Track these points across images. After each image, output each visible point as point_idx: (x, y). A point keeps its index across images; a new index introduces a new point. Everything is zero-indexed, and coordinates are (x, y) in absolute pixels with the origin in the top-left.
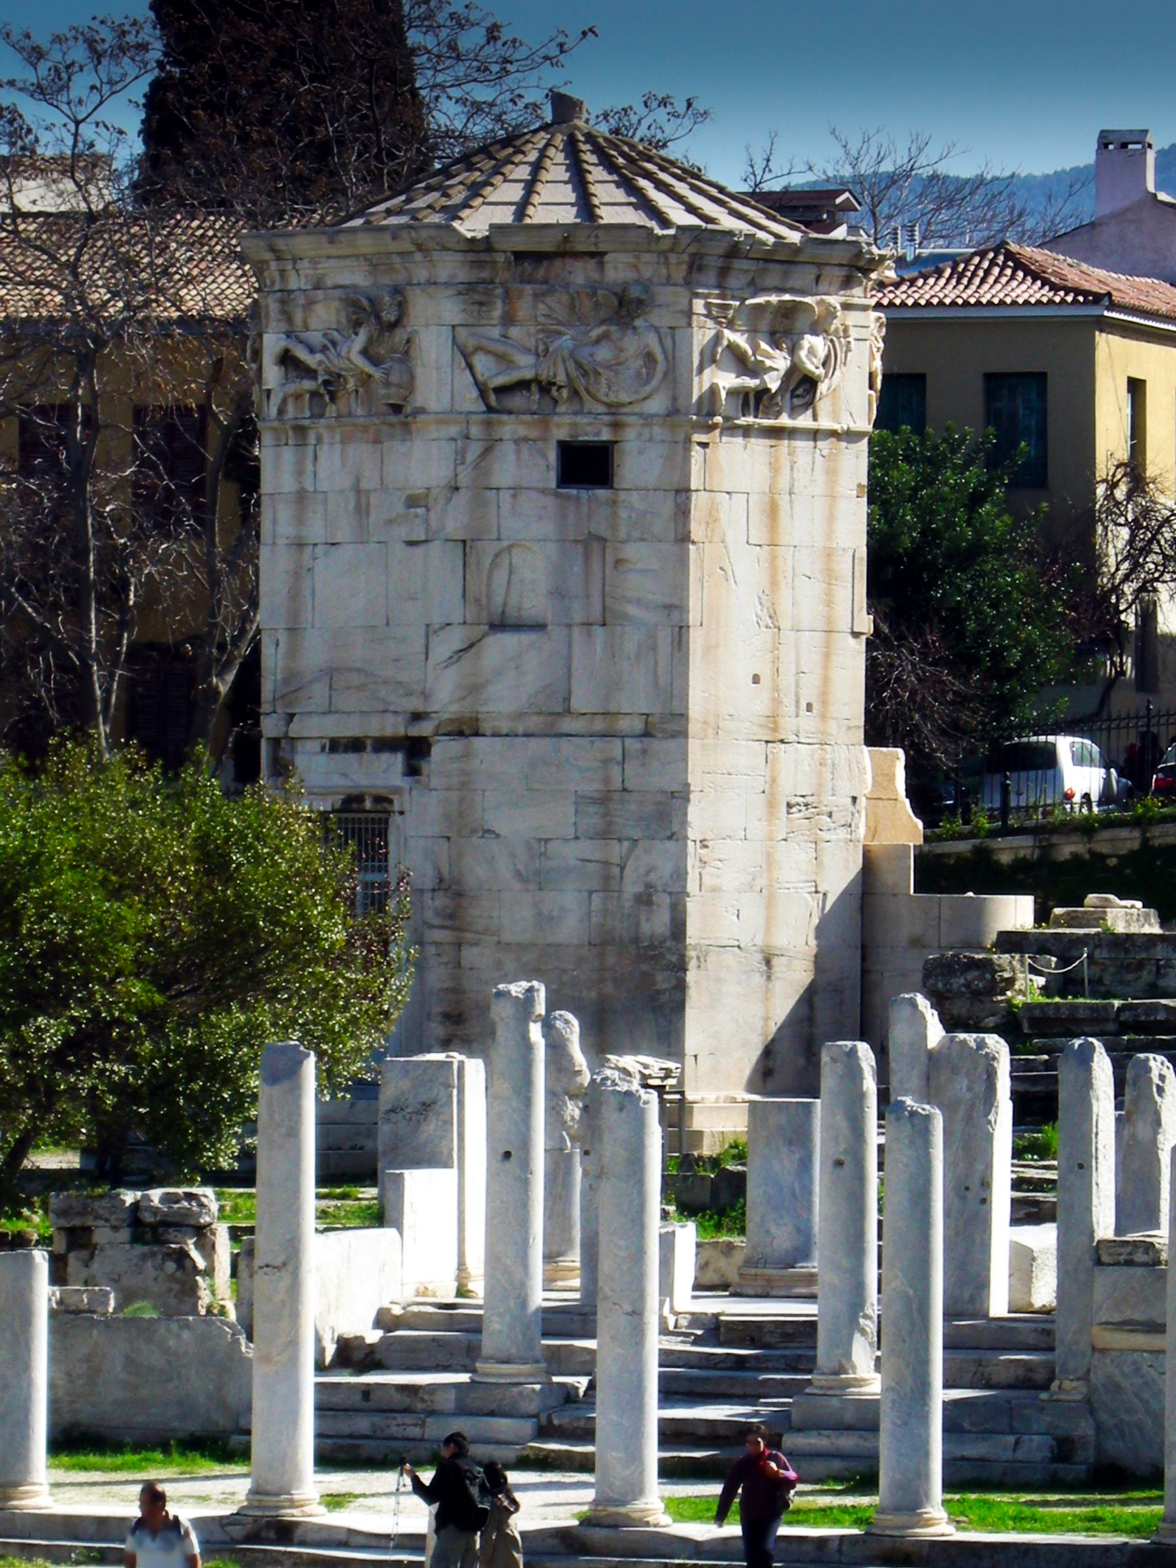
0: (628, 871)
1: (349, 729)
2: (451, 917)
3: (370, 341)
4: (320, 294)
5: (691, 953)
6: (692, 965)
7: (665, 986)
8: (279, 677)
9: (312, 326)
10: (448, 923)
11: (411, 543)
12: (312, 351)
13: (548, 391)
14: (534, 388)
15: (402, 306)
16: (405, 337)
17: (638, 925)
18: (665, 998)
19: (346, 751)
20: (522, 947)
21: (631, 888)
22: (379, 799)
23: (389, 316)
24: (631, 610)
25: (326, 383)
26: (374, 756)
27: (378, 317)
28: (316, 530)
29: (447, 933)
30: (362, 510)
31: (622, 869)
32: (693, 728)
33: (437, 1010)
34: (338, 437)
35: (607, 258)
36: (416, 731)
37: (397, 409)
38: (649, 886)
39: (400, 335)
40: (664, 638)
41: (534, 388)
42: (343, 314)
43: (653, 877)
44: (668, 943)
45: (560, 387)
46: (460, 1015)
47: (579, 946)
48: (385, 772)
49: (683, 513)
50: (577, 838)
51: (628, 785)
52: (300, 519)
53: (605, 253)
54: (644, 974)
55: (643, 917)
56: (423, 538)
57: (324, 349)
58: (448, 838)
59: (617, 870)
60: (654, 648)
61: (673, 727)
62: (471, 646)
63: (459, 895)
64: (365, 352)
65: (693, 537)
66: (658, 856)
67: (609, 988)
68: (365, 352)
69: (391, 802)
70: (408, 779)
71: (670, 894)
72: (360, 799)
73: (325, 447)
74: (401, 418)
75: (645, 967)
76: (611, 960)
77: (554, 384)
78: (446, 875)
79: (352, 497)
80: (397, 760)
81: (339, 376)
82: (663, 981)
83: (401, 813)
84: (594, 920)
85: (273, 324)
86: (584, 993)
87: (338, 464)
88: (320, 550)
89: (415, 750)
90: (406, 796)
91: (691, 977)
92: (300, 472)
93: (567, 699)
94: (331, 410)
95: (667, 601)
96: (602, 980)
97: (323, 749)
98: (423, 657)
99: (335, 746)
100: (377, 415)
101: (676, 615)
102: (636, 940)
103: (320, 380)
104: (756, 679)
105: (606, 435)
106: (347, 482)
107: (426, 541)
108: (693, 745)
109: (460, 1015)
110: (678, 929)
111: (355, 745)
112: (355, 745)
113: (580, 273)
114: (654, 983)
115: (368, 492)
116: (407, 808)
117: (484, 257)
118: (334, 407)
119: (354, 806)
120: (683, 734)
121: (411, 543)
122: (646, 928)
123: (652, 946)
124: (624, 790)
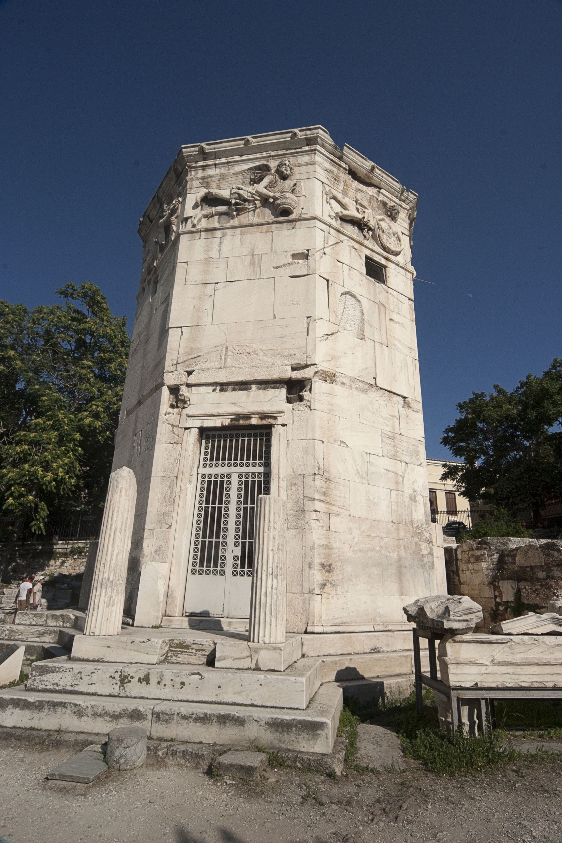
0: (405, 479)
2: (324, 494)
8: (182, 351)
10: (323, 498)
16: (292, 184)
18: (426, 560)
19: (234, 390)
20: (362, 520)
22: (263, 416)
24: (397, 343)
26: (261, 392)
29: (322, 505)
31: (403, 478)
33: (317, 561)
35: (382, 191)
36: (297, 375)
38: (415, 491)
39: (288, 184)
45: (370, 229)
46: (330, 565)
50: (383, 456)
51: (402, 432)
53: (380, 189)
54: (417, 544)
58: (323, 442)
59: (401, 479)
60: (406, 365)
62: (332, 334)
63: (328, 480)
67: (402, 553)
71: (423, 496)
72: (247, 416)
75: (416, 540)
76: (402, 534)
77: (368, 226)
78: (322, 466)
81: (245, 200)
84: (393, 507)
86: (392, 554)
89: (296, 388)
93: (375, 378)
96: (399, 546)
102: (412, 522)
105: (383, 261)
106: (245, 251)
107: (308, 275)
109: (330, 565)
111: (244, 385)
112: (244, 385)
113: (371, 191)
114: (421, 550)
117: (337, 160)
119: (241, 422)
124: (401, 434)
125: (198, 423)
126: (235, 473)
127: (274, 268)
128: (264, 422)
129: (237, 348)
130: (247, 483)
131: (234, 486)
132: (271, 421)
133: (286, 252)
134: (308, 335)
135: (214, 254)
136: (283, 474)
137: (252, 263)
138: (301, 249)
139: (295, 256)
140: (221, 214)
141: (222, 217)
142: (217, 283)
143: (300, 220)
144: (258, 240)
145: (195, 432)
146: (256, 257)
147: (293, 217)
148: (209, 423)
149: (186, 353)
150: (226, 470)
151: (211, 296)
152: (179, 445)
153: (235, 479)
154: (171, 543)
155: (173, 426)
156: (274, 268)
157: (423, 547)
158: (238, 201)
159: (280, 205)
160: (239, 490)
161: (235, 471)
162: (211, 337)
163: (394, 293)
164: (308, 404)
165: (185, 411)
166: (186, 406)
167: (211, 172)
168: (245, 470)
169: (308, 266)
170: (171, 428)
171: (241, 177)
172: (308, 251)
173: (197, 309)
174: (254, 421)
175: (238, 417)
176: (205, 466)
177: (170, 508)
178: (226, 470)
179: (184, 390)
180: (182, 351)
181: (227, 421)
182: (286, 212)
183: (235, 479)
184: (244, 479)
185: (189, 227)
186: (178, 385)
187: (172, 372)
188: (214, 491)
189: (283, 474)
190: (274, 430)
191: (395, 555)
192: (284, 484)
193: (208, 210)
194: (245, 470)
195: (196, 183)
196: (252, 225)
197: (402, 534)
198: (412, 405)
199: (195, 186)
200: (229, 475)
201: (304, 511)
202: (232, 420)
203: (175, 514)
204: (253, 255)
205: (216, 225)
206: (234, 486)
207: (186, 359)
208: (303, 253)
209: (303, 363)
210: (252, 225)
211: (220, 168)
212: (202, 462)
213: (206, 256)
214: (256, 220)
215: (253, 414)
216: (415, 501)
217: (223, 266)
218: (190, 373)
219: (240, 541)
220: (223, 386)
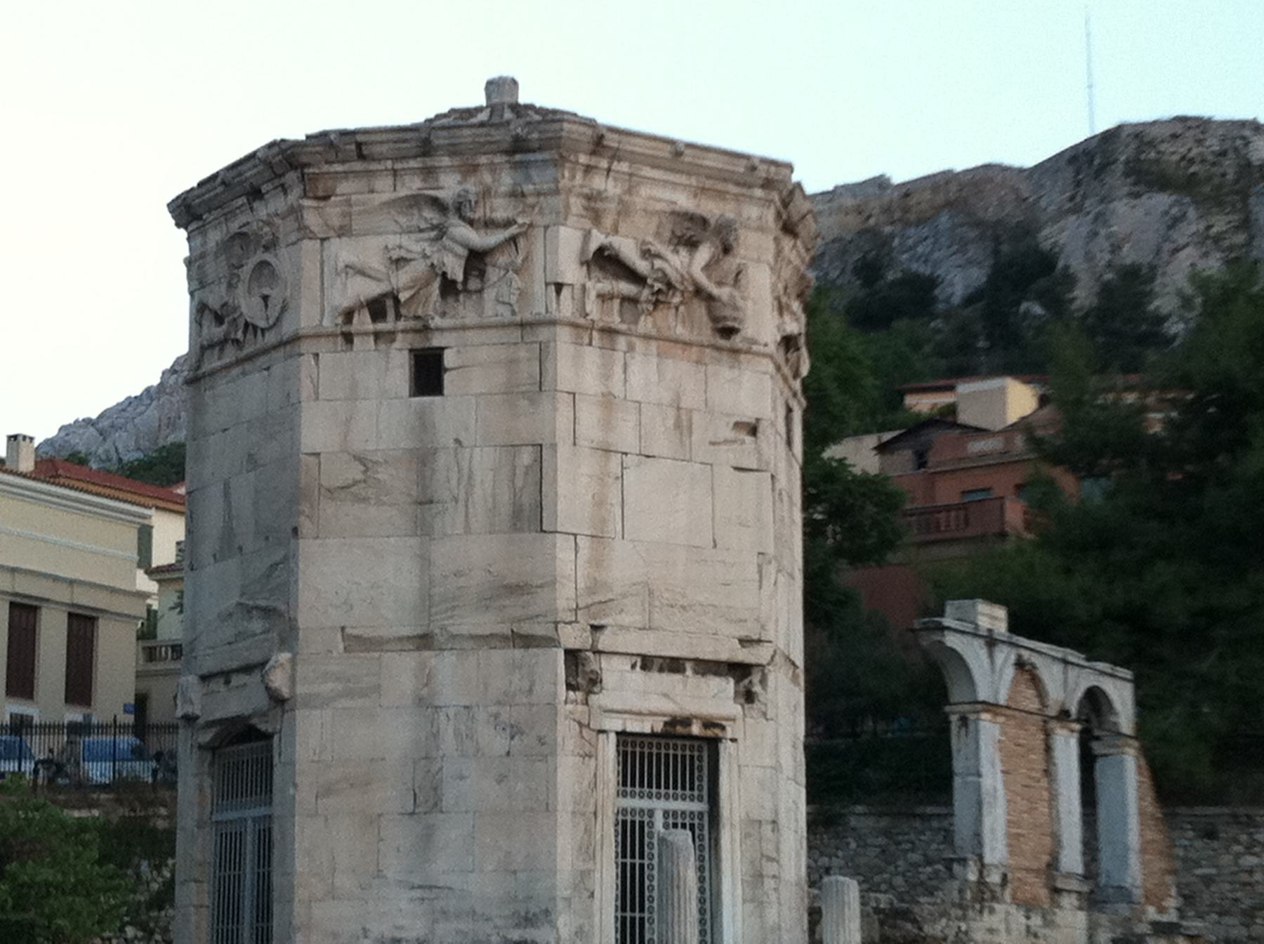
8: (581, 585)
19: (661, 670)
22: (708, 724)
26: (699, 679)
28: (626, 437)
30: (682, 427)
48: (713, 698)
52: (607, 424)
56: (755, 467)
69: (723, 728)
72: (687, 721)
73: (638, 358)
79: (671, 413)
80: (728, 686)
83: (734, 740)
85: (572, 220)
87: (655, 378)
88: (628, 460)
90: (739, 722)
92: (606, 376)
97: (633, 666)
98: (757, 584)
99: (647, 662)
106: (667, 397)
107: (757, 470)
111: (674, 665)
112: (674, 665)
115: (690, 411)
116: (739, 736)
119: (679, 729)
125: (615, 724)
127: (713, 443)
128: (709, 733)
129: (666, 595)
132: (717, 731)
133: (728, 415)
134: (760, 587)
135: (618, 389)
136: (736, 819)
137: (678, 426)
138: (749, 417)
139: (738, 425)
140: (628, 300)
141: (626, 304)
142: (626, 454)
143: (748, 352)
144: (680, 369)
145: (613, 737)
146: (683, 412)
147: (737, 341)
148: (634, 726)
149: (591, 590)
150: (644, 804)
151: (617, 478)
152: (593, 759)
154: (597, 919)
155: (580, 724)
156: (713, 443)
159: (725, 318)
162: (624, 566)
164: (763, 708)
165: (593, 699)
166: (596, 689)
167: (598, 182)
169: (759, 452)
170: (577, 726)
171: (655, 220)
172: (758, 420)
173: (600, 502)
174: (696, 729)
175: (674, 722)
176: (625, 795)
177: (590, 865)
178: (644, 804)
179: (593, 663)
180: (581, 585)
181: (659, 728)
182: (728, 332)
185: (566, 307)
186: (580, 650)
187: (570, 623)
188: (632, 835)
189: (736, 819)
190: (722, 747)
192: (737, 837)
193: (606, 285)
195: (576, 204)
196: (676, 341)
199: (574, 210)
200: (651, 813)
201: (761, 876)
202: (666, 724)
203: (598, 875)
204: (679, 408)
205: (615, 320)
207: (590, 601)
208: (748, 424)
209: (756, 637)
210: (676, 341)
211: (615, 179)
213: (605, 390)
214: (681, 331)
215: (696, 717)
217: (632, 418)
218: (596, 628)
220: (647, 662)
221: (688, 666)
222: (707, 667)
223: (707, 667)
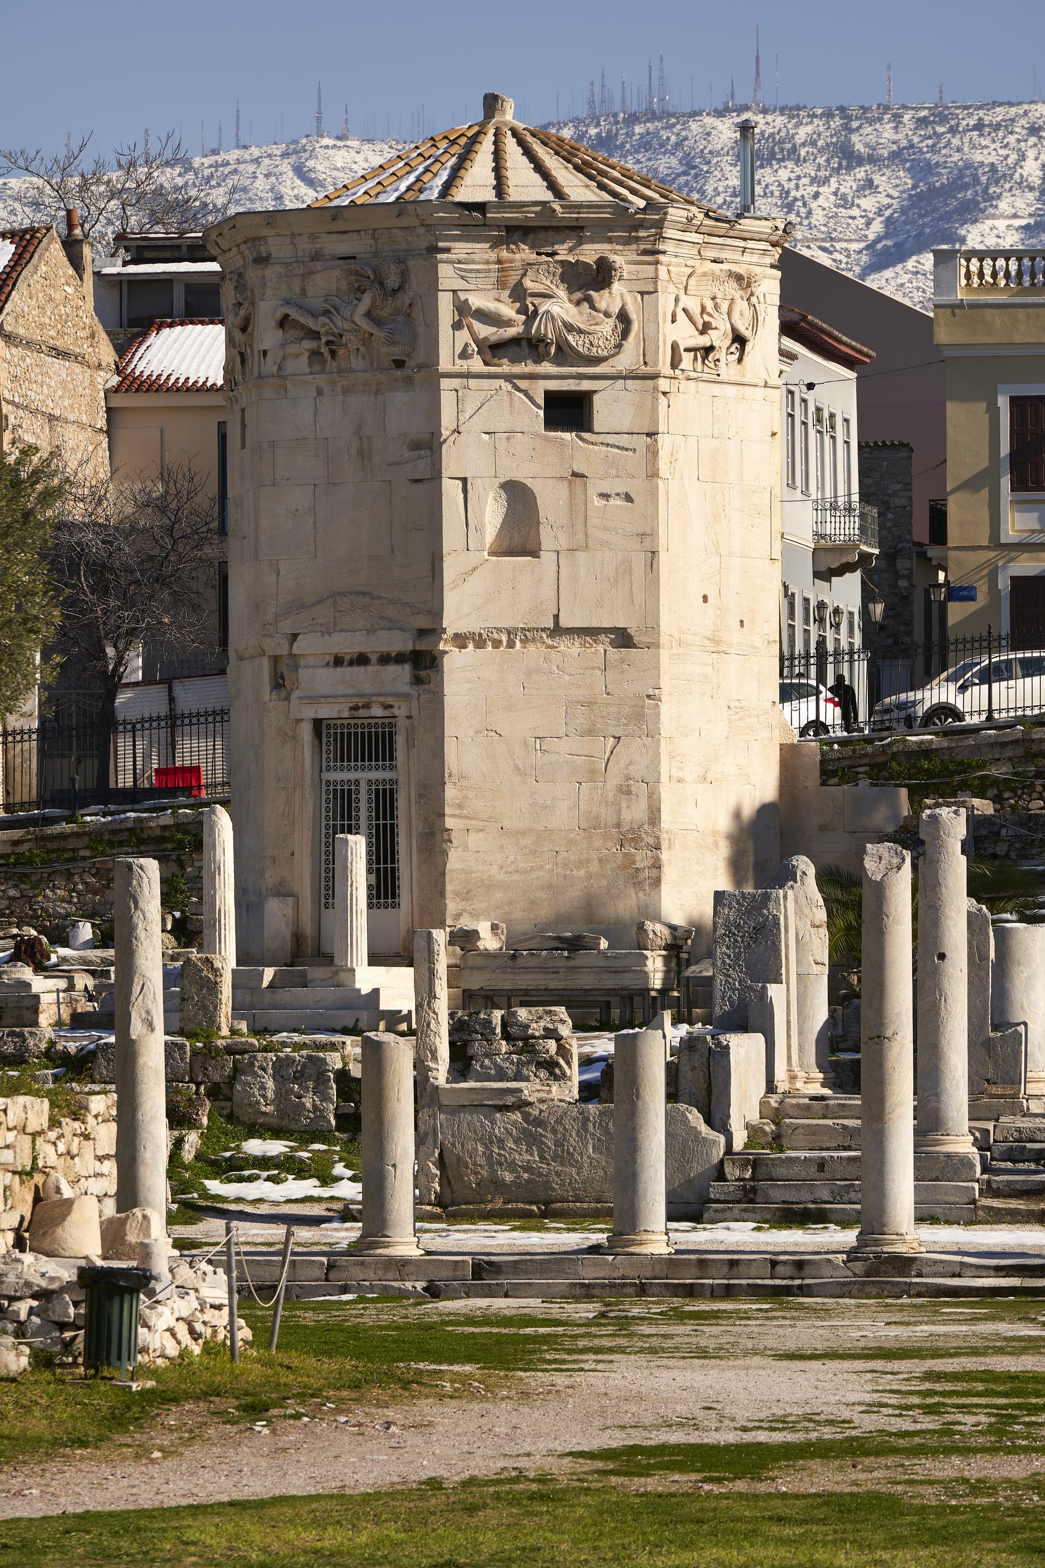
1: (351, 644)
2: (460, 806)
3: (373, 306)
4: (319, 266)
5: (664, 836)
6: (664, 845)
7: (642, 865)
9: (310, 294)
10: (458, 812)
11: (416, 481)
12: (314, 315)
13: (537, 347)
14: (524, 343)
15: (404, 274)
16: (408, 301)
17: (620, 811)
19: (351, 663)
20: (523, 833)
21: (613, 781)
23: (392, 282)
25: (328, 343)
27: (381, 284)
29: (457, 820)
32: (664, 640)
34: (339, 390)
36: (422, 646)
37: (399, 364)
39: (404, 299)
40: (639, 560)
41: (524, 343)
42: (344, 282)
43: (632, 771)
44: (646, 827)
47: (570, 831)
49: (653, 453)
55: (624, 805)
57: (326, 313)
61: (646, 639)
64: (368, 315)
65: (661, 474)
66: (632, 751)
68: (368, 315)
70: (416, 687)
74: (406, 372)
82: (642, 858)
89: (424, 663)
91: (665, 856)
93: (556, 617)
94: (331, 365)
95: (641, 531)
100: (379, 369)
101: (647, 541)
102: (618, 825)
103: (324, 340)
104: (705, 598)
108: (664, 653)
110: (654, 817)
111: (362, 660)
112: (362, 660)
114: (634, 863)
116: (415, 713)
118: (335, 364)
120: (657, 646)
121: (416, 481)
122: (627, 815)
123: (632, 830)
125: (310, 713)
126: (365, 777)
128: (387, 713)
130: (377, 790)
131: (363, 796)
150: (352, 776)
153: (363, 788)
157: (638, 858)
158: (331, 338)
160: (369, 801)
161: (363, 776)
163: (610, 439)
168: (374, 775)
178: (352, 776)
183: (363, 788)
184: (373, 788)
191: (582, 872)
194: (374, 775)
197: (597, 843)
198: (636, 640)
206: (363, 796)
212: (324, 764)
216: (629, 793)
219: (374, 866)
221: (374, 658)
222: (385, 659)
223: (385, 659)
